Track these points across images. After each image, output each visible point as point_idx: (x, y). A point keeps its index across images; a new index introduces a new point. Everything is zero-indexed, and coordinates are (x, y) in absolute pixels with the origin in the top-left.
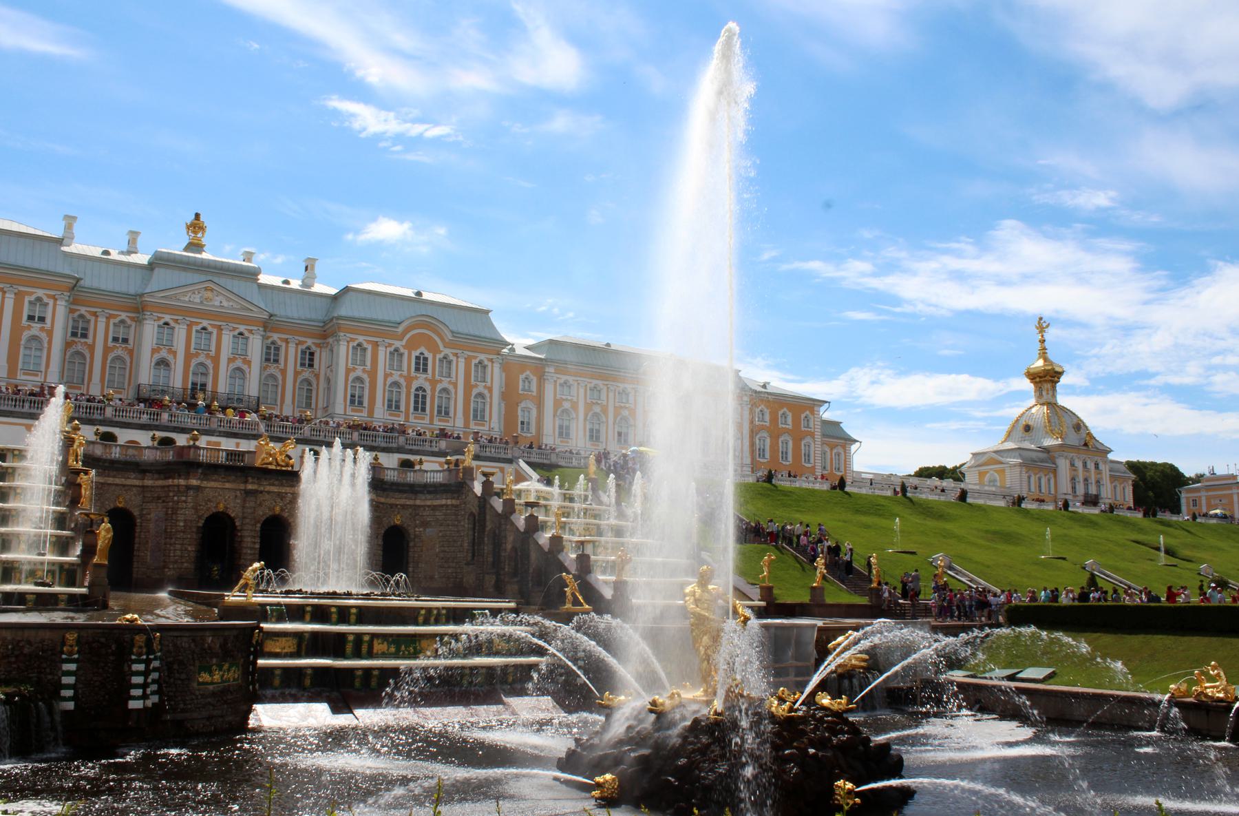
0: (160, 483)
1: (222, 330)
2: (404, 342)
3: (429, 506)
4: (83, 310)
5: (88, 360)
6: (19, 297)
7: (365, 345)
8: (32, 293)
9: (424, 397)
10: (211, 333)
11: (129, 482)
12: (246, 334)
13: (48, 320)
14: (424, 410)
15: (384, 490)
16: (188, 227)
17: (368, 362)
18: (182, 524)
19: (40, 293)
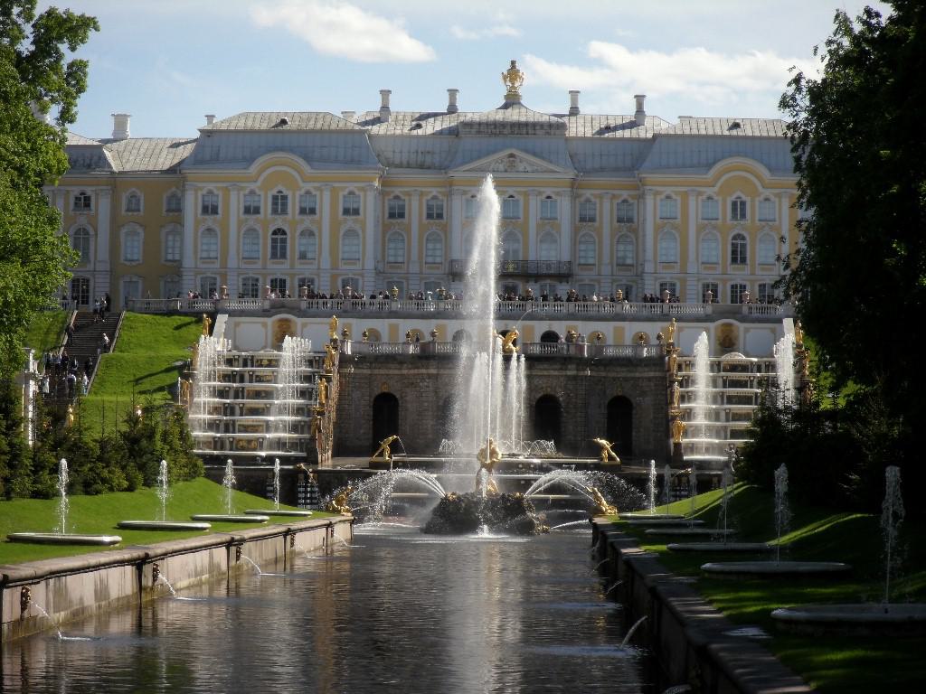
0: (412, 372)
1: (529, 195)
2: (716, 189)
3: (646, 378)
4: (397, 191)
5: (406, 239)
6: (334, 191)
7: (674, 196)
8: (344, 188)
9: (743, 246)
10: (518, 201)
11: (391, 372)
12: (554, 196)
13: (361, 211)
14: (743, 260)
15: (605, 366)
16: (505, 78)
17: (679, 216)
18: (426, 404)
19: (352, 187)
